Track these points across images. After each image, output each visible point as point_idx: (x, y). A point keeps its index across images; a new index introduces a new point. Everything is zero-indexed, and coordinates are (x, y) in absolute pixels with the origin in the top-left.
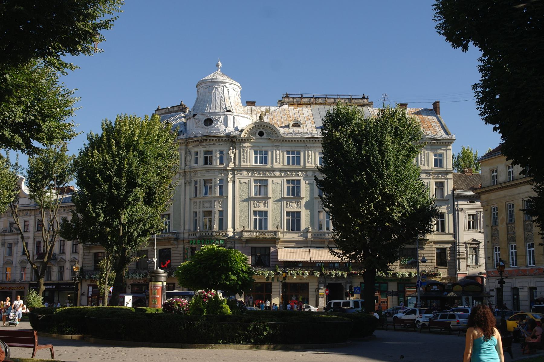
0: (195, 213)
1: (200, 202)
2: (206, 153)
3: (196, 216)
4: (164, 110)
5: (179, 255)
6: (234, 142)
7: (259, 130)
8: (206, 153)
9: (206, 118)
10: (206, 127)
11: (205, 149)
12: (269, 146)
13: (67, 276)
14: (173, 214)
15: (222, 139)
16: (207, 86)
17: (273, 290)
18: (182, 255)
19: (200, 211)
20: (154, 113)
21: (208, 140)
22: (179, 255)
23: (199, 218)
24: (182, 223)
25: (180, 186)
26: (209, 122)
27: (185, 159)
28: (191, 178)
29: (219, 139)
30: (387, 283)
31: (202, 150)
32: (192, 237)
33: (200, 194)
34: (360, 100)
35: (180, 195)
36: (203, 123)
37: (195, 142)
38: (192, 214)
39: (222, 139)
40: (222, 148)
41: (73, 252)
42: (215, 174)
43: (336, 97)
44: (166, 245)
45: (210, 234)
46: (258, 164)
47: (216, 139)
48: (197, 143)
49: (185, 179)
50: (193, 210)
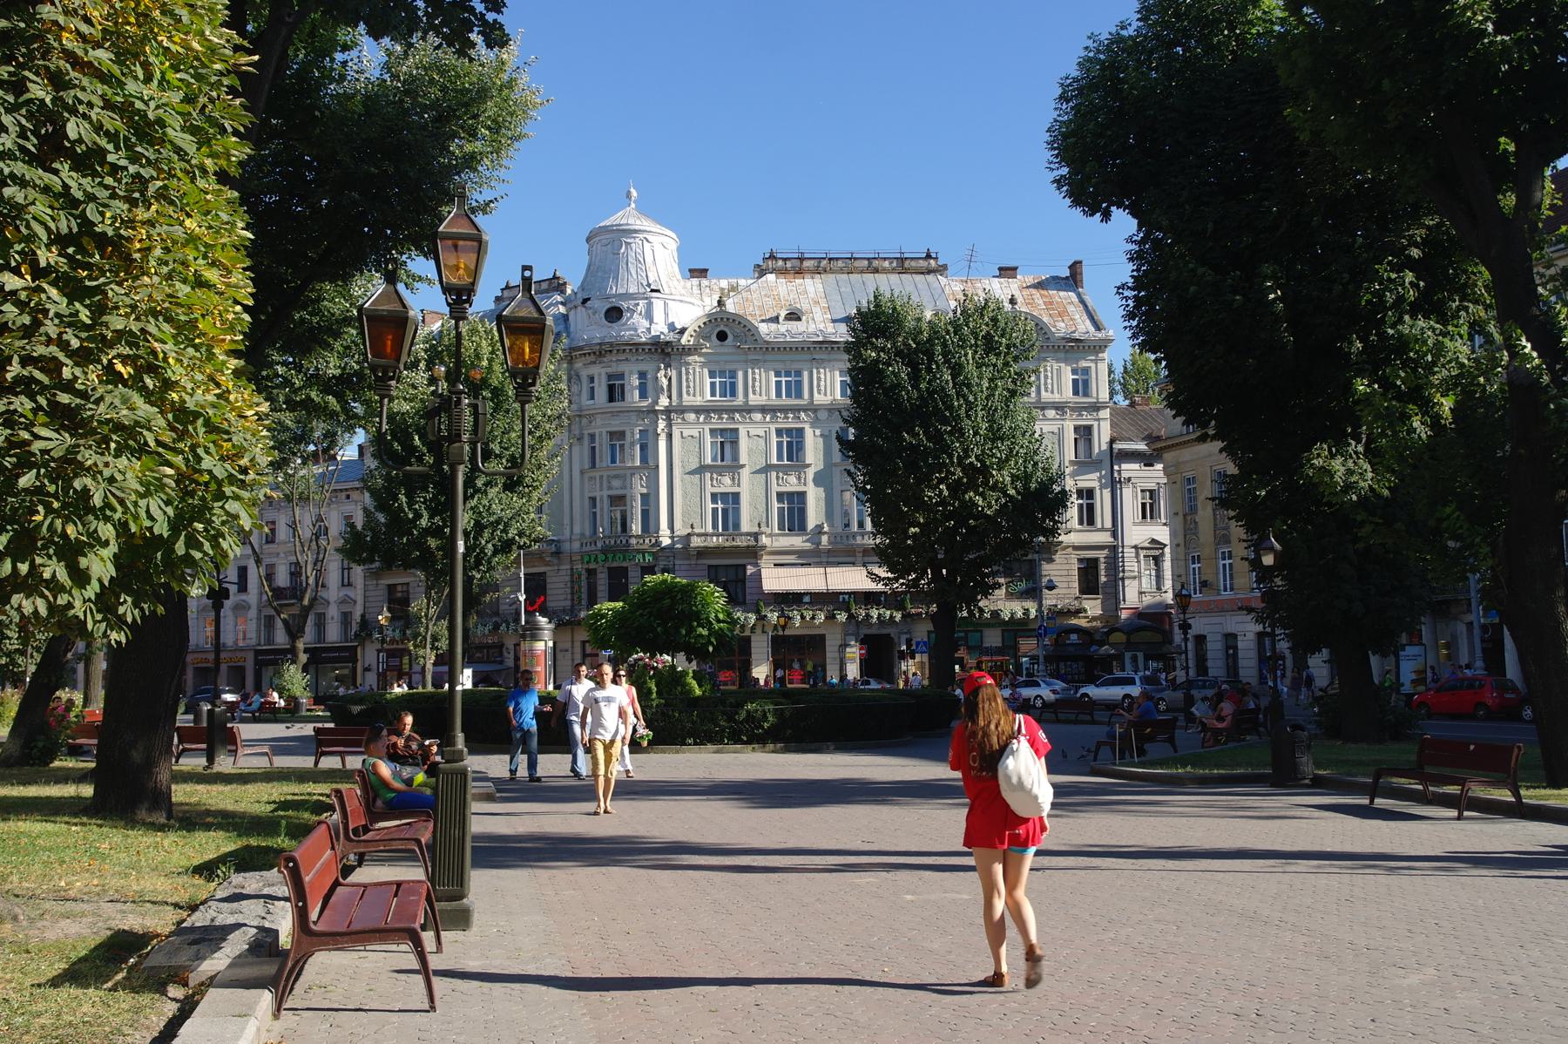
0: (593, 500)
1: (601, 477)
2: (610, 377)
3: (595, 506)
5: (562, 585)
6: (668, 354)
7: (718, 330)
8: (610, 377)
9: (609, 306)
10: (610, 324)
11: (609, 370)
12: (738, 362)
13: (333, 634)
15: (643, 350)
17: (753, 650)
18: (569, 585)
19: (603, 494)
20: (500, 294)
22: (562, 585)
23: (602, 509)
24: (567, 521)
26: (615, 314)
28: (581, 429)
29: (637, 350)
30: (981, 631)
31: (604, 371)
32: (588, 548)
33: (601, 461)
34: (921, 261)
36: (602, 315)
38: (587, 501)
39: (643, 350)
40: (642, 367)
41: (343, 585)
43: (872, 256)
45: (624, 542)
46: (718, 398)
48: (592, 358)
50: (588, 495)
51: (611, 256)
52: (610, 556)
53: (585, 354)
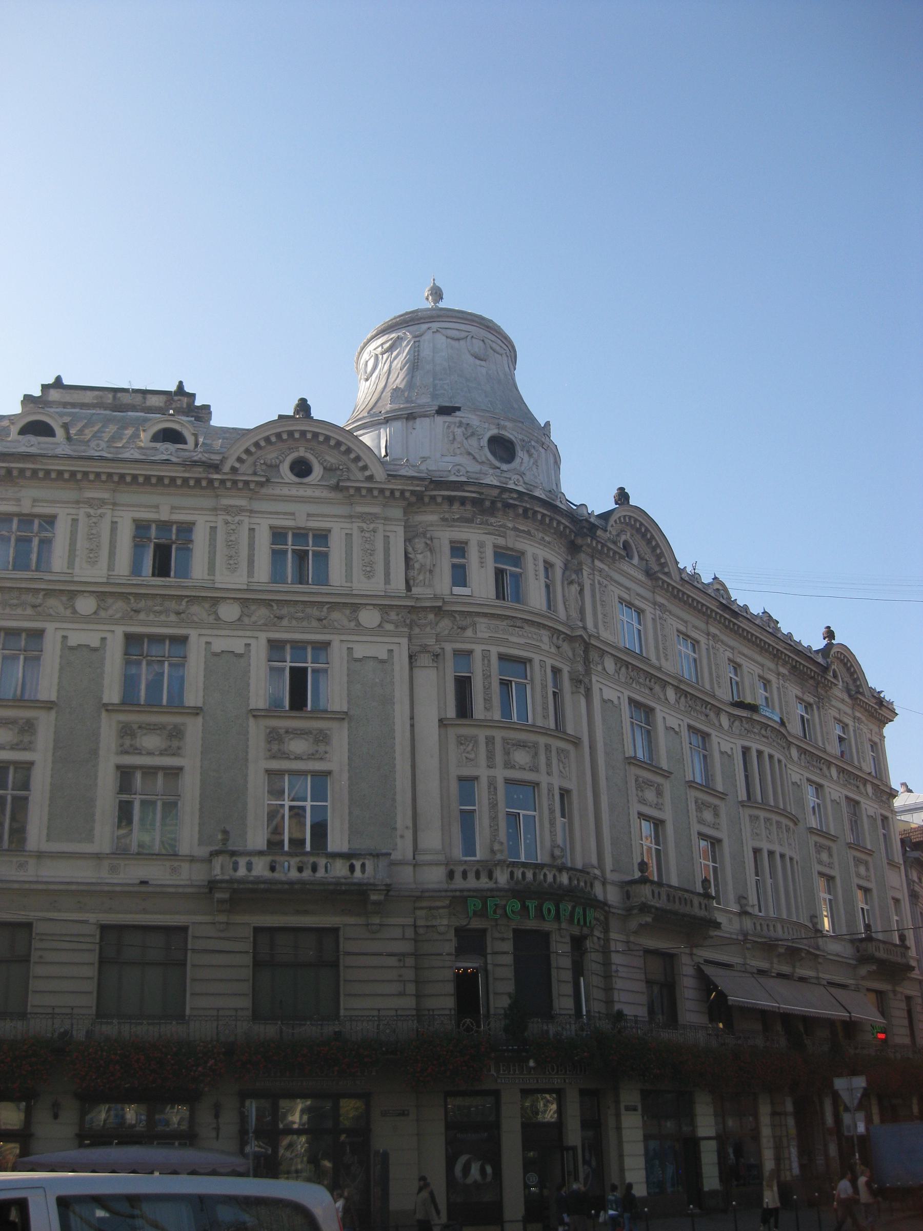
4: (89, 393)
9: (494, 431)
10: (497, 464)
11: (501, 541)
14: (346, 776)
16: (465, 334)
20: (37, 393)
21: (521, 511)
24: (403, 819)
25: (383, 662)
27: (407, 559)
32: (472, 883)
35: (387, 701)
36: (484, 442)
37: (456, 506)
38: (454, 786)
39: (559, 523)
42: (541, 641)
44: (306, 912)
45: (550, 878)
47: (544, 515)
49: (410, 639)
50: (454, 771)
51: (471, 360)
52: (531, 905)
53: (450, 500)
